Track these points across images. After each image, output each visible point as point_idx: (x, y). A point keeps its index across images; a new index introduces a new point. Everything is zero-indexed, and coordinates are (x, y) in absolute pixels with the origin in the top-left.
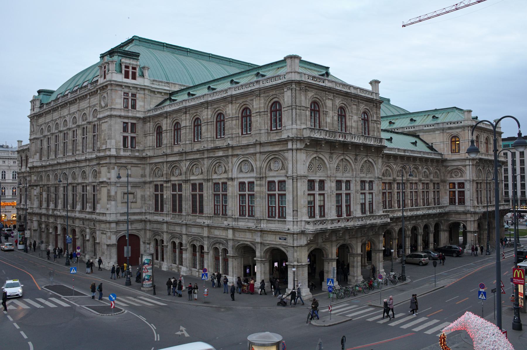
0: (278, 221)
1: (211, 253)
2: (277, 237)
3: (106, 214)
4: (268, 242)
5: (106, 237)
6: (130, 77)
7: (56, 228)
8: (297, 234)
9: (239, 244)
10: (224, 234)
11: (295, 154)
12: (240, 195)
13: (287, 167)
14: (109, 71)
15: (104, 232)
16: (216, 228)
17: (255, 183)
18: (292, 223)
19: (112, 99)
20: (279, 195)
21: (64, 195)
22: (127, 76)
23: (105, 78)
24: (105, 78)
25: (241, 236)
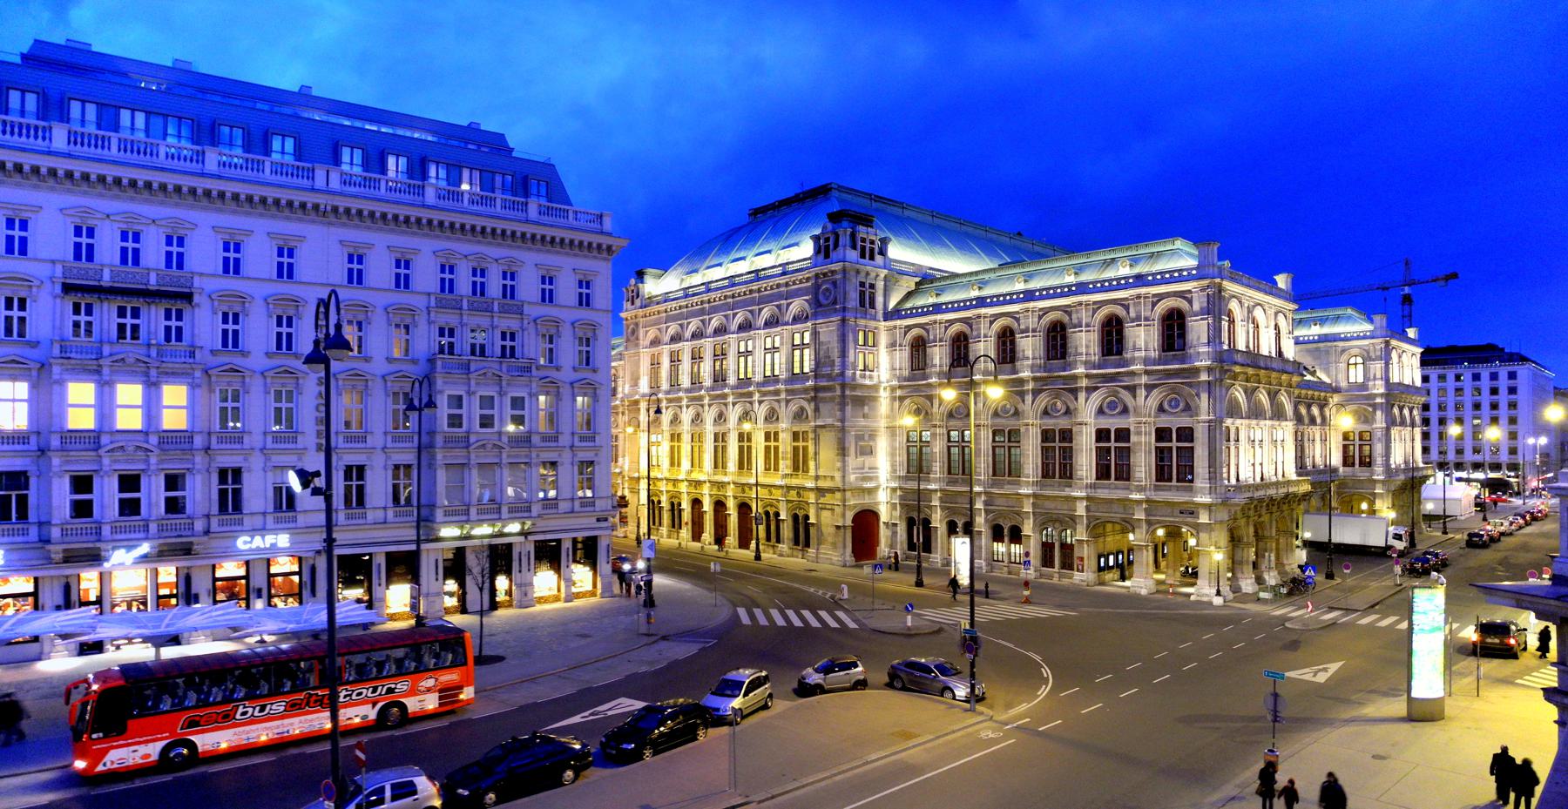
1: (1038, 535)
3: (832, 477)
5: (833, 515)
6: (867, 256)
7: (696, 503)
8: (1216, 505)
10: (1065, 507)
12: (1097, 447)
13: (1198, 407)
14: (836, 246)
15: (828, 507)
16: (1048, 498)
17: (1132, 429)
19: (845, 294)
20: (1178, 448)
21: (716, 447)
22: (863, 256)
23: (827, 256)
24: (827, 256)
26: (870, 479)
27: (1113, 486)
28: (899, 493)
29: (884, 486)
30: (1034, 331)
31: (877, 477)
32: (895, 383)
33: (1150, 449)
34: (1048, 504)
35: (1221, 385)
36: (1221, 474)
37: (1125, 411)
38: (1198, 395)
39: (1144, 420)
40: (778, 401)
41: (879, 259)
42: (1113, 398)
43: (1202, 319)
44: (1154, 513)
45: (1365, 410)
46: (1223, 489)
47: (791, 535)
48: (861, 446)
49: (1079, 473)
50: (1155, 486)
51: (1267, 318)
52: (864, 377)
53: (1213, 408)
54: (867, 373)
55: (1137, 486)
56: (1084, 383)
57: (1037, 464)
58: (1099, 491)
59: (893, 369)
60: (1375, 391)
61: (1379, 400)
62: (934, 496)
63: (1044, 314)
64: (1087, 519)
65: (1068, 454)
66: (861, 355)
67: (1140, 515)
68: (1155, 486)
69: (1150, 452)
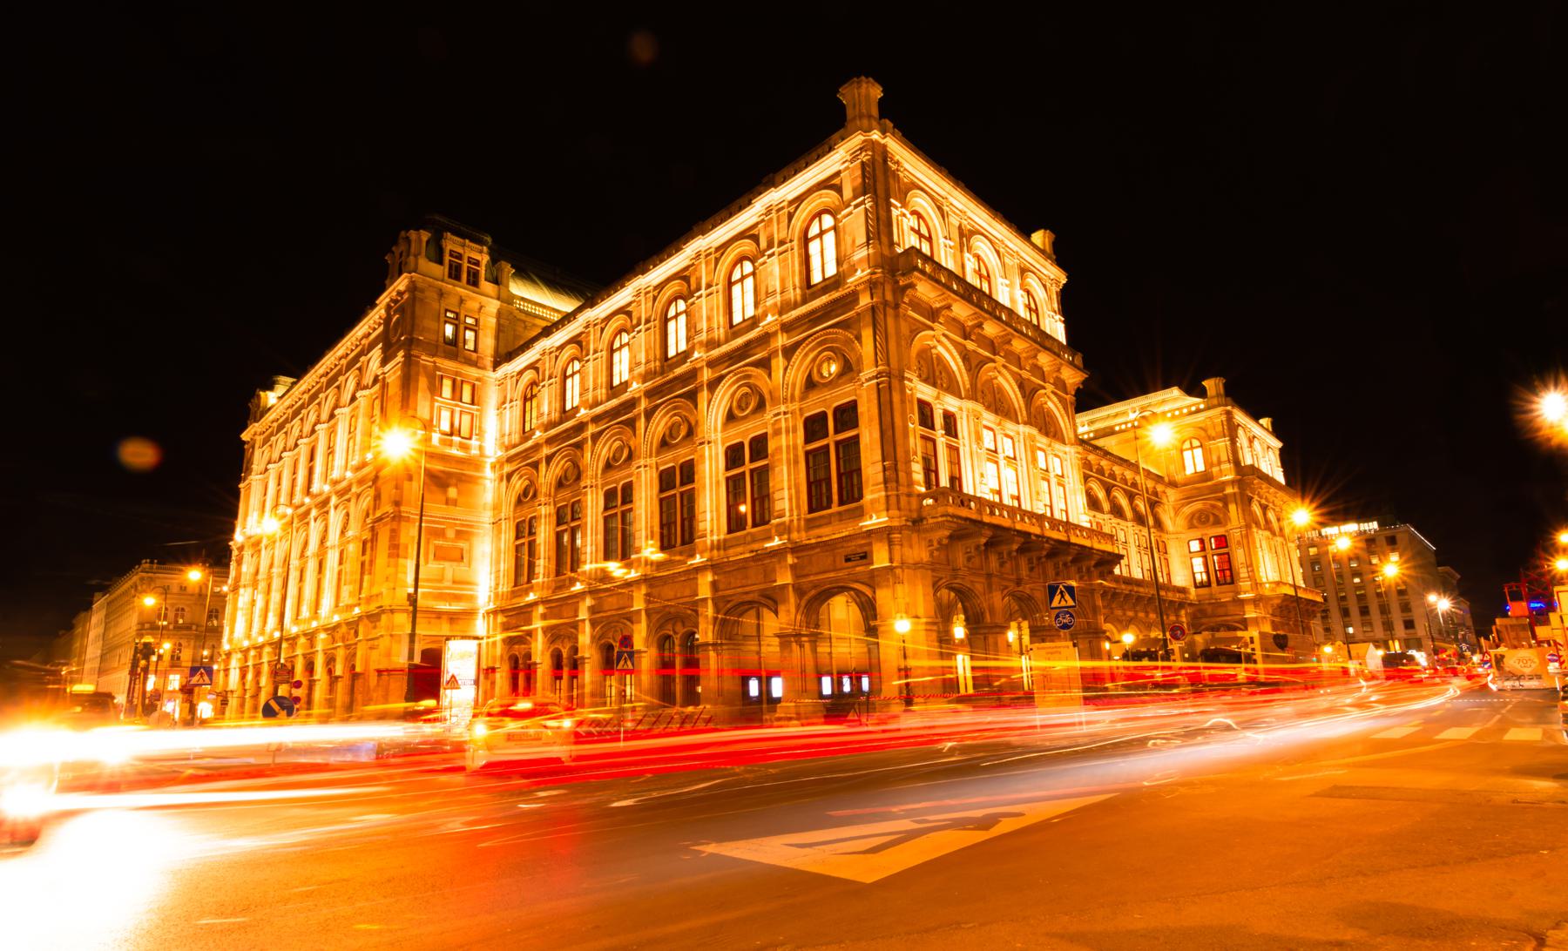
0: (839, 513)
2: (838, 559)
4: (812, 578)
8: (900, 529)
9: (729, 606)
11: (882, 316)
13: (859, 360)
18: (883, 500)
25: (733, 586)
26: (458, 598)
27: (749, 538)
28: (500, 619)
29: (482, 611)
30: (647, 321)
31: (471, 598)
32: (500, 453)
33: (796, 456)
34: (668, 592)
35: (897, 316)
36: (909, 473)
37: (761, 406)
38: (859, 338)
39: (783, 408)
40: (349, 500)
41: (487, 286)
42: (746, 390)
43: (856, 206)
44: (805, 572)
45: (1213, 506)
46: (914, 502)
47: (347, 699)
48: (437, 548)
49: (701, 526)
50: (807, 521)
51: (1004, 265)
52: (451, 444)
53: (881, 352)
54: (456, 439)
55: (779, 525)
56: (706, 375)
57: (652, 527)
58: (731, 551)
59: (503, 436)
60: (1224, 478)
61: (1229, 490)
62: (534, 614)
63: (659, 293)
64: (715, 605)
65: (690, 500)
66: (446, 415)
67: (784, 578)
68: (807, 521)
69: (796, 462)
